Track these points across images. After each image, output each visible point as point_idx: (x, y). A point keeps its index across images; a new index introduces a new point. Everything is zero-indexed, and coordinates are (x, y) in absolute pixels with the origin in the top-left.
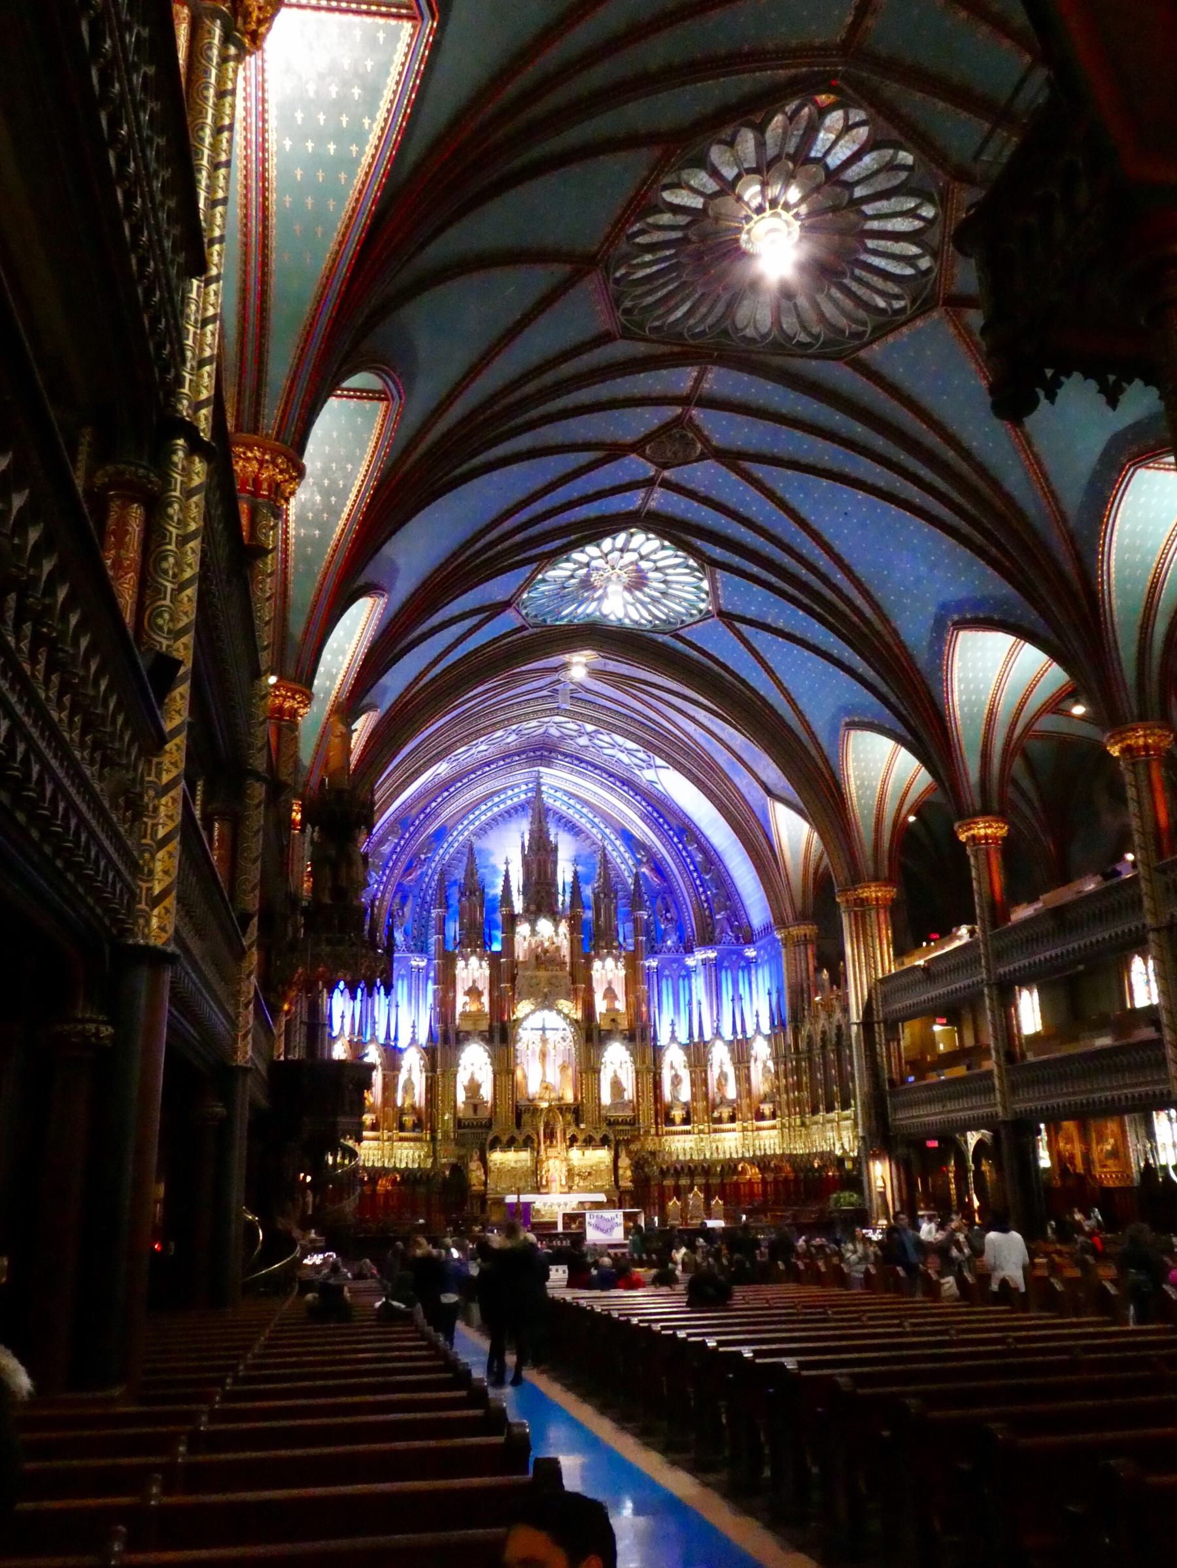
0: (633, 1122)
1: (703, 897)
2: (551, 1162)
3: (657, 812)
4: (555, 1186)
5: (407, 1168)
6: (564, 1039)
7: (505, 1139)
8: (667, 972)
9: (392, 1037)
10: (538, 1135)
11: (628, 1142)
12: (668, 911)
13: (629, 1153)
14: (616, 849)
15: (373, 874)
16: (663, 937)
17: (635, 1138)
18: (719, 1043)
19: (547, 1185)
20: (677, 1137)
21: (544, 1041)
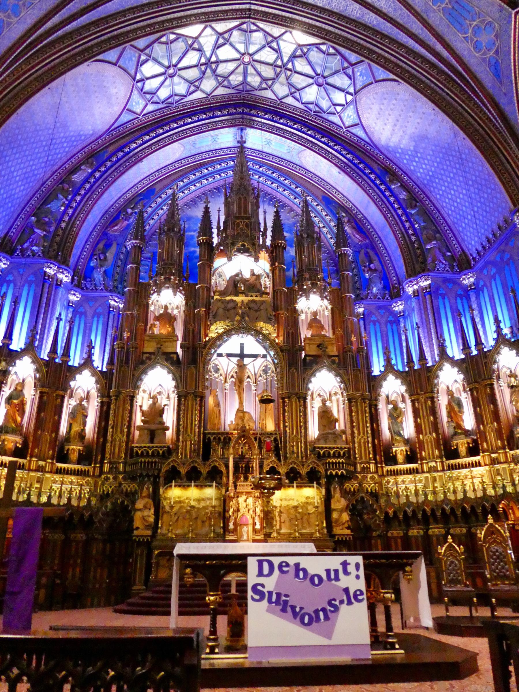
0: (349, 455)
1: (410, 232)
2: (241, 499)
3: (358, 158)
4: (247, 531)
5: (49, 503)
6: (265, 371)
7: (183, 471)
8: (373, 318)
9: (60, 351)
10: (227, 467)
11: (343, 479)
12: (371, 262)
13: (345, 493)
14: (318, 214)
15: (61, 197)
16: (367, 284)
17: (349, 477)
18: (447, 366)
19: (235, 530)
20: (400, 478)
21: (241, 367)
